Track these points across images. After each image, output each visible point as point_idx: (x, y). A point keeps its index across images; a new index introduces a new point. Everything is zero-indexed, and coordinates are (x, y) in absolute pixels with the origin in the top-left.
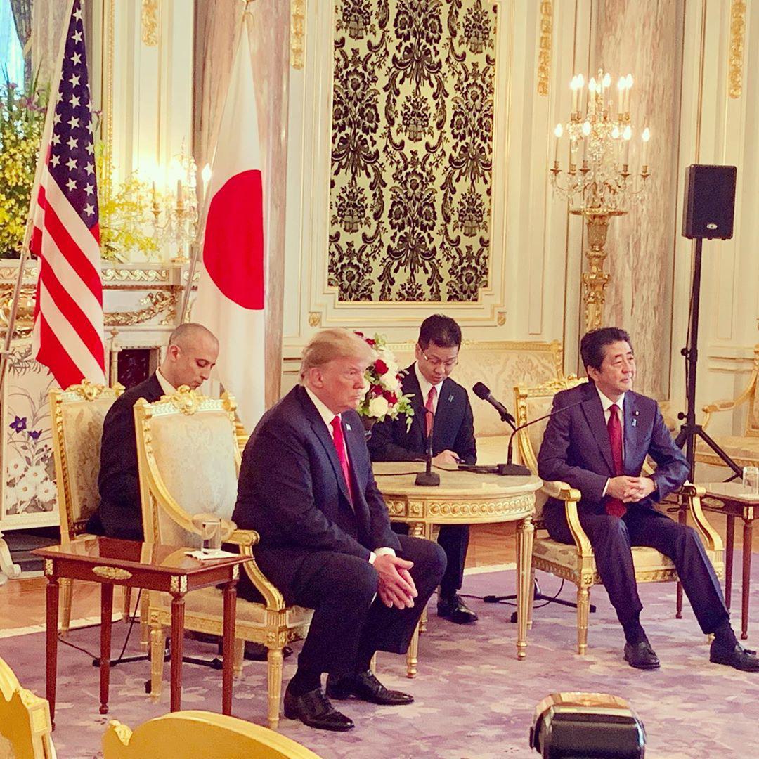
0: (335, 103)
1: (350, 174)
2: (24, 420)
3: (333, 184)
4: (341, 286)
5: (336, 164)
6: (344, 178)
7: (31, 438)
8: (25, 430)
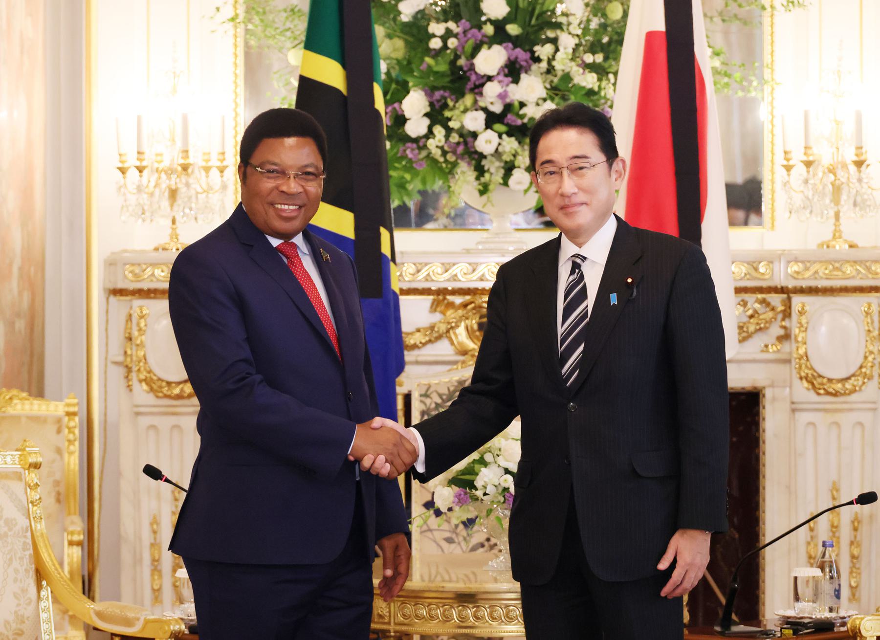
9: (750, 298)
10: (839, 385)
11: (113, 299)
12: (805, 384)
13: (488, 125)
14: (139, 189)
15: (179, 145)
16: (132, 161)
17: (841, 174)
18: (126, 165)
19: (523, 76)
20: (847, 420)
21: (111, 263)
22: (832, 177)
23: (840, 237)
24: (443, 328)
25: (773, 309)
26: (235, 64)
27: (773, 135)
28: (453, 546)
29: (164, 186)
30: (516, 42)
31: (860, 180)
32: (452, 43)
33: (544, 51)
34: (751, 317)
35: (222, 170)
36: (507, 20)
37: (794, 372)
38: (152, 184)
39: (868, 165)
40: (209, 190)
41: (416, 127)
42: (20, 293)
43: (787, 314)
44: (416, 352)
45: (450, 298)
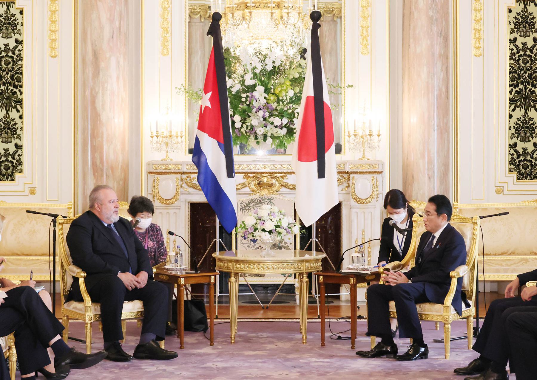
0: (510, 73)
1: (523, 111)
3: (511, 116)
4: (519, 172)
5: (513, 106)
6: (519, 113)
7: (252, 242)
9: (339, 175)
10: (365, 201)
11: (149, 175)
14: (157, 142)
15: (169, 129)
16: (155, 134)
17: (365, 138)
18: (153, 135)
21: (148, 164)
22: (362, 139)
23: (365, 157)
25: (345, 178)
26: (185, 106)
27: (345, 127)
29: (164, 142)
31: (371, 140)
35: (181, 137)
37: (351, 197)
38: (161, 141)
39: (373, 136)
40: (178, 143)
42: (121, 173)
43: (349, 179)
45: (249, 175)
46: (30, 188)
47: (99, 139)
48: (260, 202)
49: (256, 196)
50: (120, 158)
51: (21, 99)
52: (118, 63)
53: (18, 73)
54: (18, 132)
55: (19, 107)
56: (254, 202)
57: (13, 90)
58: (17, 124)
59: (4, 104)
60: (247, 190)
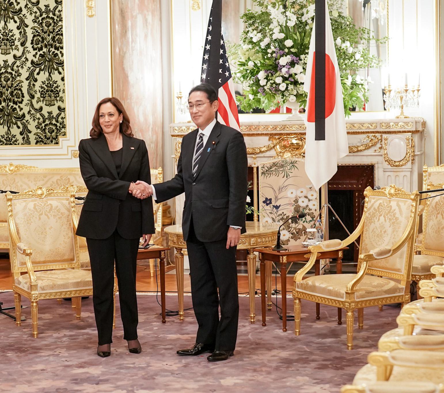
2: (270, 200)
7: (275, 209)
8: (271, 205)
9: (371, 135)
10: (398, 163)
12: (387, 163)
13: (283, 82)
19: (296, 65)
20: (402, 174)
24: (272, 146)
28: (272, 215)
30: (294, 54)
32: (274, 55)
33: (302, 57)
34: (370, 141)
36: (292, 47)
41: (263, 82)
42: (152, 136)
44: (264, 153)
46: (73, 152)
47: (128, 101)
48: (282, 166)
49: (278, 160)
50: (151, 119)
51: (62, 60)
52: (146, 20)
53: (59, 34)
54: (61, 94)
55: (60, 69)
56: (276, 165)
57: (54, 52)
58: (59, 86)
59: (46, 66)
60: (272, 153)
